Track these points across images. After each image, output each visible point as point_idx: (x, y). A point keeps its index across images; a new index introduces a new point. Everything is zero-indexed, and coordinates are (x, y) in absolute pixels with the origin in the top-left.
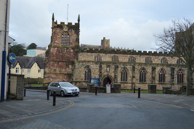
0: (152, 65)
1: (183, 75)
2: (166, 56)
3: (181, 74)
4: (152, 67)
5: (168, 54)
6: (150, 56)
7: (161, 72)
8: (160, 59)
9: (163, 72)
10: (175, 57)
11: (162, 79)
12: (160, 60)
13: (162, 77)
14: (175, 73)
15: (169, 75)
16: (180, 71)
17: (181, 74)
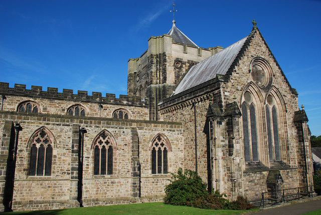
0: (6, 117)
1: (111, 148)
2: (82, 101)
3: (107, 147)
4: (6, 122)
5: (88, 97)
6: (35, 98)
7: (38, 141)
8: (64, 110)
9: (46, 141)
10: (109, 106)
11: (41, 165)
12: (66, 111)
13: (41, 159)
14: (88, 142)
15: (65, 151)
16: (104, 139)
17: (107, 147)
